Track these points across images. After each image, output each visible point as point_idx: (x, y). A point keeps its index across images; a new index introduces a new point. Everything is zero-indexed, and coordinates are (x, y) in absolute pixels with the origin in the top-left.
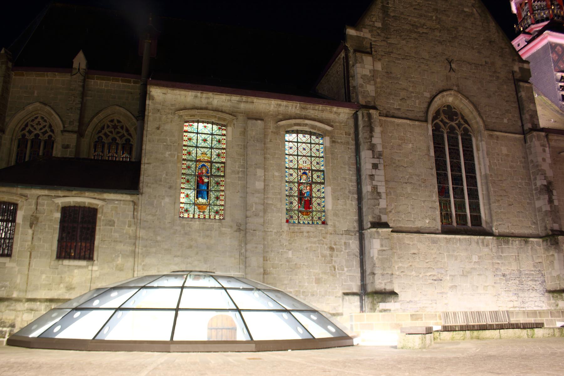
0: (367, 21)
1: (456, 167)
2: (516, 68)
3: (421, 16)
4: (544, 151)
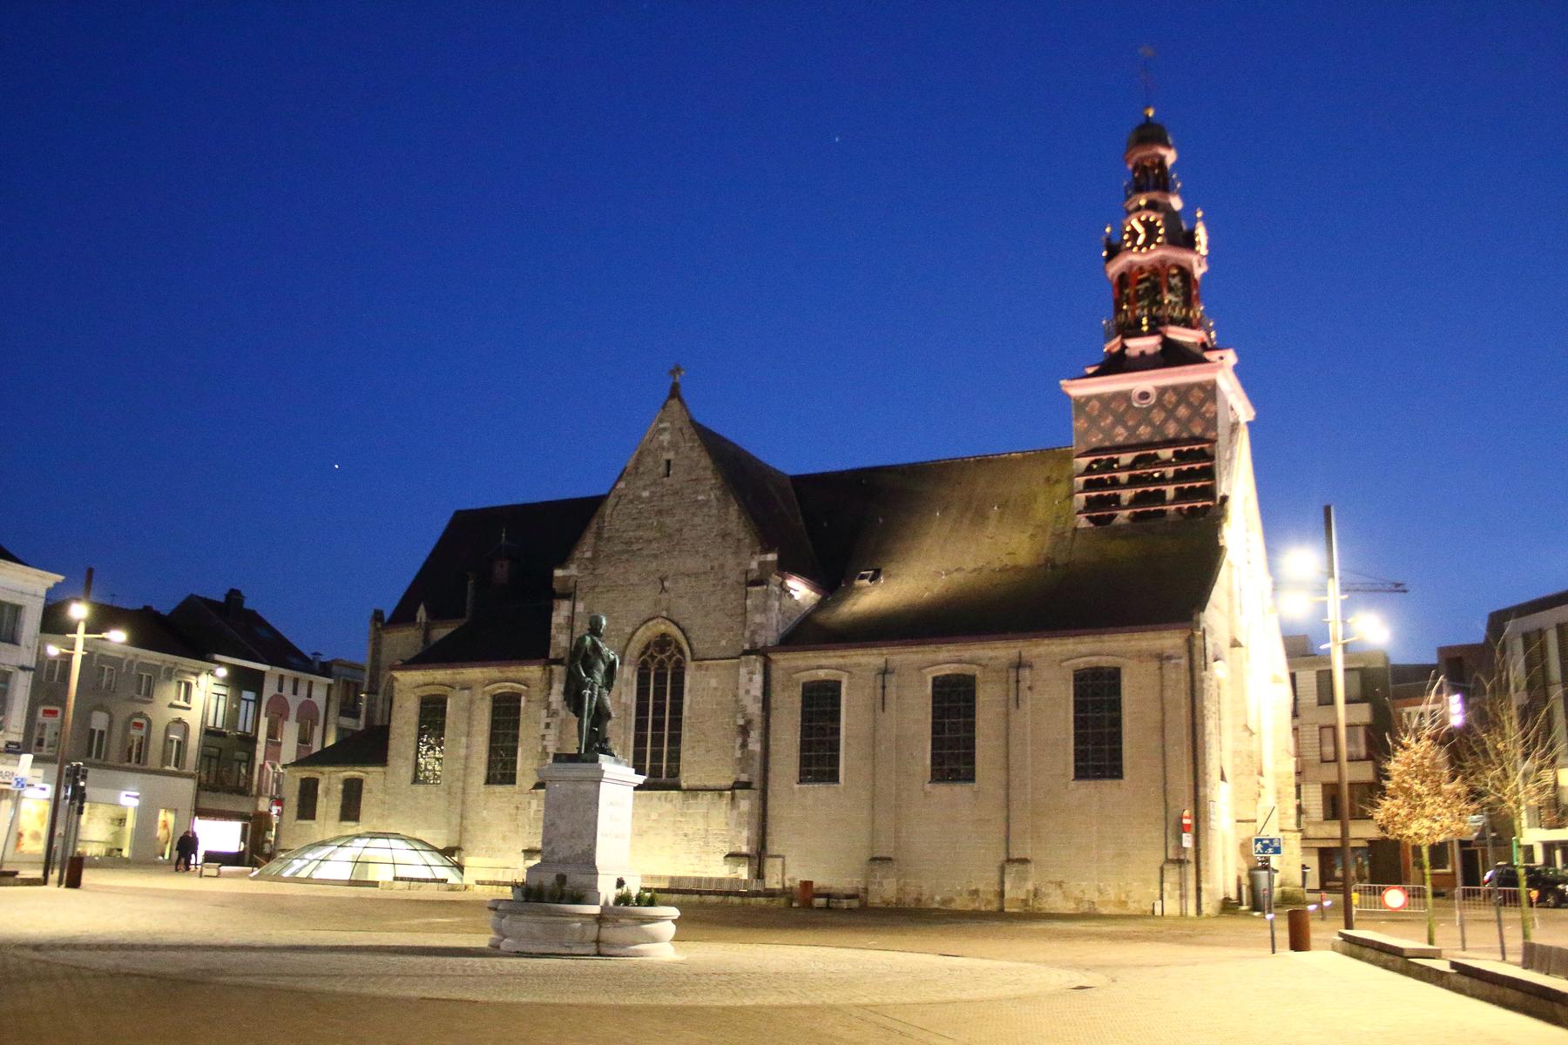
0: (577, 554)
1: (659, 709)
2: (754, 565)
3: (639, 527)
4: (751, 680)
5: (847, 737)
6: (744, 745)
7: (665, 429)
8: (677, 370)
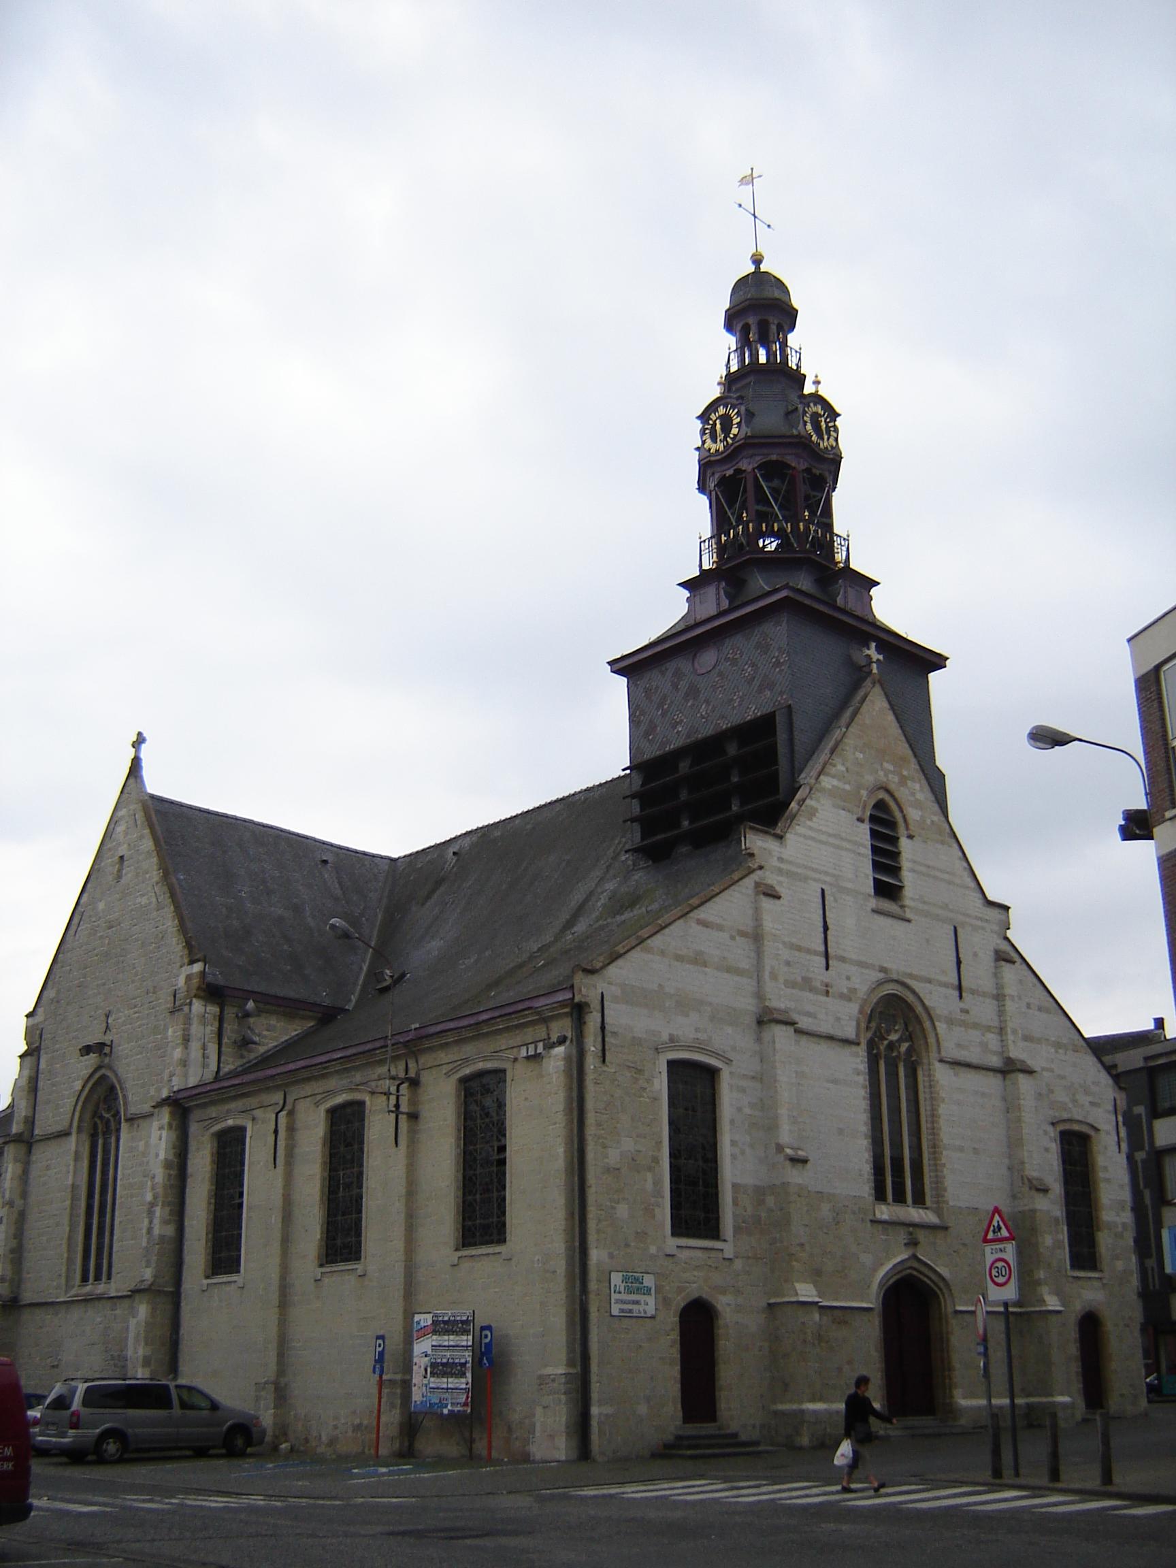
2: (181, 981)
5: (249, 1208)
6: (150, 1230)
7: (121, 818)
8: (139, 741)
